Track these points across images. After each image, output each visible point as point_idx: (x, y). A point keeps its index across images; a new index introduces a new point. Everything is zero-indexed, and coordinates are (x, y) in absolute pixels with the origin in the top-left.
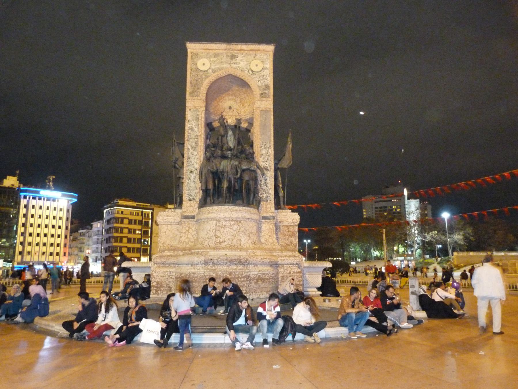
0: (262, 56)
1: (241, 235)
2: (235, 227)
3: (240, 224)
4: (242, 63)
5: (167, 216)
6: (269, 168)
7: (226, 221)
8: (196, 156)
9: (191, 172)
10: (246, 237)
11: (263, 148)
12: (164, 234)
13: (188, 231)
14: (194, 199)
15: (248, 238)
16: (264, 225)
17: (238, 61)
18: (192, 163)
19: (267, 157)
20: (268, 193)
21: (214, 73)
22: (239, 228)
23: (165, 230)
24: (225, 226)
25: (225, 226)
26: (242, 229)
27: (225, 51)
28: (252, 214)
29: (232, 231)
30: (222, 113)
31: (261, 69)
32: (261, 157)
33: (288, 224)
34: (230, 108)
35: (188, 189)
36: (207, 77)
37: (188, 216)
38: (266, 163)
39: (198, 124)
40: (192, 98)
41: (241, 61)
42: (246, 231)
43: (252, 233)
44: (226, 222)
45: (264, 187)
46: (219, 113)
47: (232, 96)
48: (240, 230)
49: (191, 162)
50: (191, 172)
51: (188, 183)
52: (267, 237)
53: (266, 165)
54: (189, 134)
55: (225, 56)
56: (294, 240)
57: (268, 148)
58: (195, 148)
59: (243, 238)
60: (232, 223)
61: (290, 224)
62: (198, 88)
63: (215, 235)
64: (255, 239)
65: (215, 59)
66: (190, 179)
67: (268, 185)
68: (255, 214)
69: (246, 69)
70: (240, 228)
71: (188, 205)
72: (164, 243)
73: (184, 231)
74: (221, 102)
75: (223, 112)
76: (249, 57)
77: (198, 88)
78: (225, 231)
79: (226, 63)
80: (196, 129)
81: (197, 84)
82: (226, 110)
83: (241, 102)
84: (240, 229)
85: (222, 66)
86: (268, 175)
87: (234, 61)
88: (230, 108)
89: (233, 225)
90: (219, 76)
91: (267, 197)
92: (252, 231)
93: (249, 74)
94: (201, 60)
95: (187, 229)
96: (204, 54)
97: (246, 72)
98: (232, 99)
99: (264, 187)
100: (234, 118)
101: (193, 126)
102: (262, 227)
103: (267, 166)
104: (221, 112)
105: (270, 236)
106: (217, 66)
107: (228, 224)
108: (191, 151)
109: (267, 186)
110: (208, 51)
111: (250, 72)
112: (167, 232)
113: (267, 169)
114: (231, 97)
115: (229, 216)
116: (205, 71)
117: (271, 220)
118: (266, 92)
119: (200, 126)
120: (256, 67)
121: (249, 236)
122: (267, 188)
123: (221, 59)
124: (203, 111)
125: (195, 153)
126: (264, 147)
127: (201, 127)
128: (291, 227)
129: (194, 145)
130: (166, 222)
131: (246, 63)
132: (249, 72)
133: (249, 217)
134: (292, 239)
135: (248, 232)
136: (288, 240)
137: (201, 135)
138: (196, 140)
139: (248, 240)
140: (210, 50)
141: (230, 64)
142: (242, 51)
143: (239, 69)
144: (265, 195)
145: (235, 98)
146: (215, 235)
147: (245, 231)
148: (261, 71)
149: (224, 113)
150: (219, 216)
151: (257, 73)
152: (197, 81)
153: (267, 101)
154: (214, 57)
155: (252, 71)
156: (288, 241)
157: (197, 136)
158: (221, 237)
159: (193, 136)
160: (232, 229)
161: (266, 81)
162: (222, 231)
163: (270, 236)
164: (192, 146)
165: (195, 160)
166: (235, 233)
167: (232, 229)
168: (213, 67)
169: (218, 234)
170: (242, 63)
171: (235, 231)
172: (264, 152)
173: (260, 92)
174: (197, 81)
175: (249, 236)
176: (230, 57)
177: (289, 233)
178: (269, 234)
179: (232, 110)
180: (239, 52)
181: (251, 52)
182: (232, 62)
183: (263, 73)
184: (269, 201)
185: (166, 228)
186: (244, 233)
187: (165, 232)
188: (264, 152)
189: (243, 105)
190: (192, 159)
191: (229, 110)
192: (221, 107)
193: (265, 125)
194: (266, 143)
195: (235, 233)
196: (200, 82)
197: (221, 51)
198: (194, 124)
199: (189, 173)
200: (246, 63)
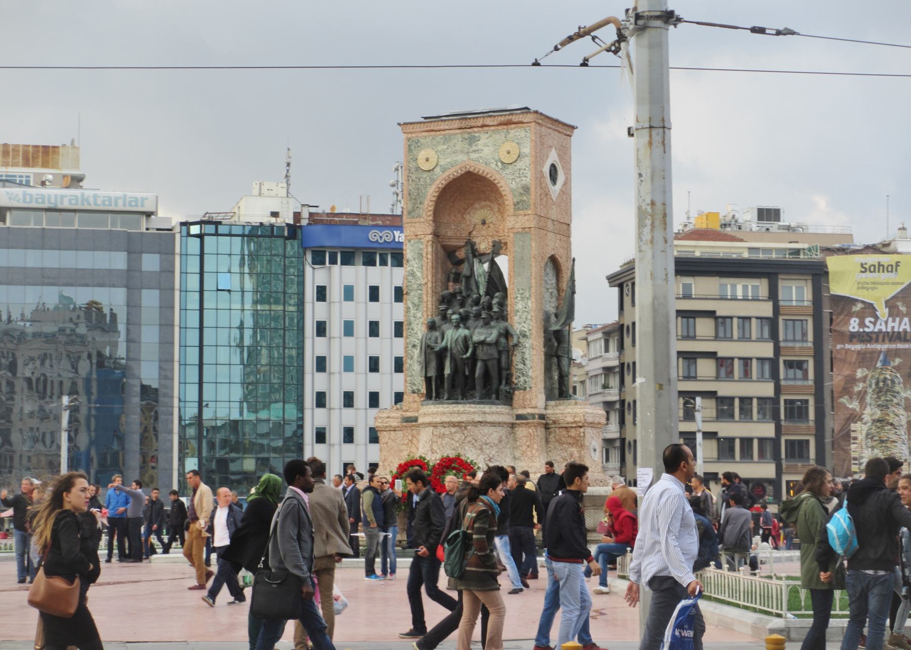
0: (517, 134)
1: (467, 448)
2: (458, 436)
3: (465, 432)
4: (486, 150)
5: (388, 417)
6: (528, 333)
7: (445, 427)
8: (421, 320)
9: (414, 346)
10: (474, 451)
11: (519, 299)
12: (385, 445)
13: (411, 441)
14: (419, 390)
15: (479, 452)
16: (521, 429)
17: (480, 147)
18: (415, 331)
19: (526, 314)
20: (527, 376)
21: (443, 172)
22: (463, 437)
23: (387, 440)
24: (444, 435)
25: (444, 435)
26: (469, 439)
27: (459, 131)
28: (487, 415)
29: (453, 442)
30: (470, 233)
31: (515, 157)
32: (516, 315)
33: (567, 426)
34: (484, 223)
35: (410, 374)
36: (433, 180)
37: (410, 417)
38: (523, 324)
39: (422, 265)
40: (411, 220)
41: (486, 145)
42: (476, 441)
43: (486, 444)
44: (444, 429)
45: (521, 366)
46: (465, 234)
47: (485, 201)
48: (466, 441)
49: (413, 330)
50: (414, 346)
51: (410, 365)
52: (524, 448)
53: (523, 329)
54: (410, 284)
55: (460, 139)
56: (575, 452)
57: (527, 298)
58: (418, 306)
59: (469, 452)
60: (453, 430)
61: (571, 425)
62: (421, 203)
63: (432, 449)
64: (493, 452)
65: (445, 147)
66: (412, 358)
67: (527, 362)
68: (493, 413)
69: (493, 161)
70: (466, 437)
71: (411, 399)
72: (385, 460)
73: (407, 441)
74: (469, 213)
75: (472, 231)
76: (497, 137)
77: (421, 203)
78: (444, 442)
79: (462, 152)
80: (419, 274)
81: (418, 195)
82: (477, 226)
83: (499, 209)
84: (464, 439)
85: (455, 159)
86: (527, 345)
87: (474, 148)
88: (484, 223)
89: (455, 432)
90: (452, 177)
91: (526, 382)
92: (488, 441)
93: (497, 169)
94: (423, 152)
95: (410, 437)
96: (428, 140)
97: (493, 166)
98: (486, 206)
99: (521, 366)
100: (490, 240)
101: (415, 270)
102: (518, 433)
103: (526, 330)
104: (467, 233)
105: (528, 446)
106: (449, 160)
107: (446, 431)
108: (412, 311)
109: (524, 364)
110: (433, 133)
111: (499, 164)
112: (390, 442)
113: (525, 336)
114: (484, 203)
115: (448, 420)
116: (429, 171)
117: (529, 421)
118: (525, 198)
119: (424, 268)
120: (508, 156)
121: (481, 449)
122: (526, 368)
123: (455, 145)
124: (428, 241)
125: (419, 315)
126: (522, 298)
127: (427, 270)
128: (573, 430)
129: (416, 301)
130: (387, 427)
131: (492, 149)
132: (497, 165)
133: (480, 420)
134: (572, 449)
135: (480, 443)
136: (566, 451)
137: (426, 284)
138: (420, 292)
139: (478, 456)
140: (436, 131)
141: (468, 153)
142: (486, 128)
143: (481, 161)
144: (522, 379)
145: (490, 204)
146: (432, 449)
147: (474, 441)
148: (515, 161)
149: (474, 233)
150: (435, 420)
151: (510, 166)
152: (418, 189)
153: (525, 215)
154: (444, 144)
155: (503, 163)
156: (566, 454)
157: (421, 285)
158: (438, 451)
159: (415, 286)
160: (453, 439)
161: (524, 178)
162: (439, 443)
163: (528, 446)
164: (413, 303)
165: (419, 326)
166: (458, 445)
167: (453, 439)
168: (442, 162)
169: (435, 447)
170: (486, 150)
171: (458, 441)
172: (520, 306)
173: (515, 200)
174: (418, 189)
175: (481, 449)
176: (467, 141)
177: (570, 440)
178: (528, 443)
179: (486, 226)
180: (480, 129)
181: (500, 128)
182: (470, 150)
183: (520, 164)
184: (528, 389)
185: (387, 436)
186: (473, 444)
187: (387, 443)
188: (520, 307)
189: (502, 217)
190: (414, 326)
191: (481, 226)
192: (468, 223)
193: (522, 258)
194: (523, 289)
195: (458, 445)
196: (424, 191)
197: (454, 132)
198: (416, 265)
199: (410, 348)
200: (492, 149)
